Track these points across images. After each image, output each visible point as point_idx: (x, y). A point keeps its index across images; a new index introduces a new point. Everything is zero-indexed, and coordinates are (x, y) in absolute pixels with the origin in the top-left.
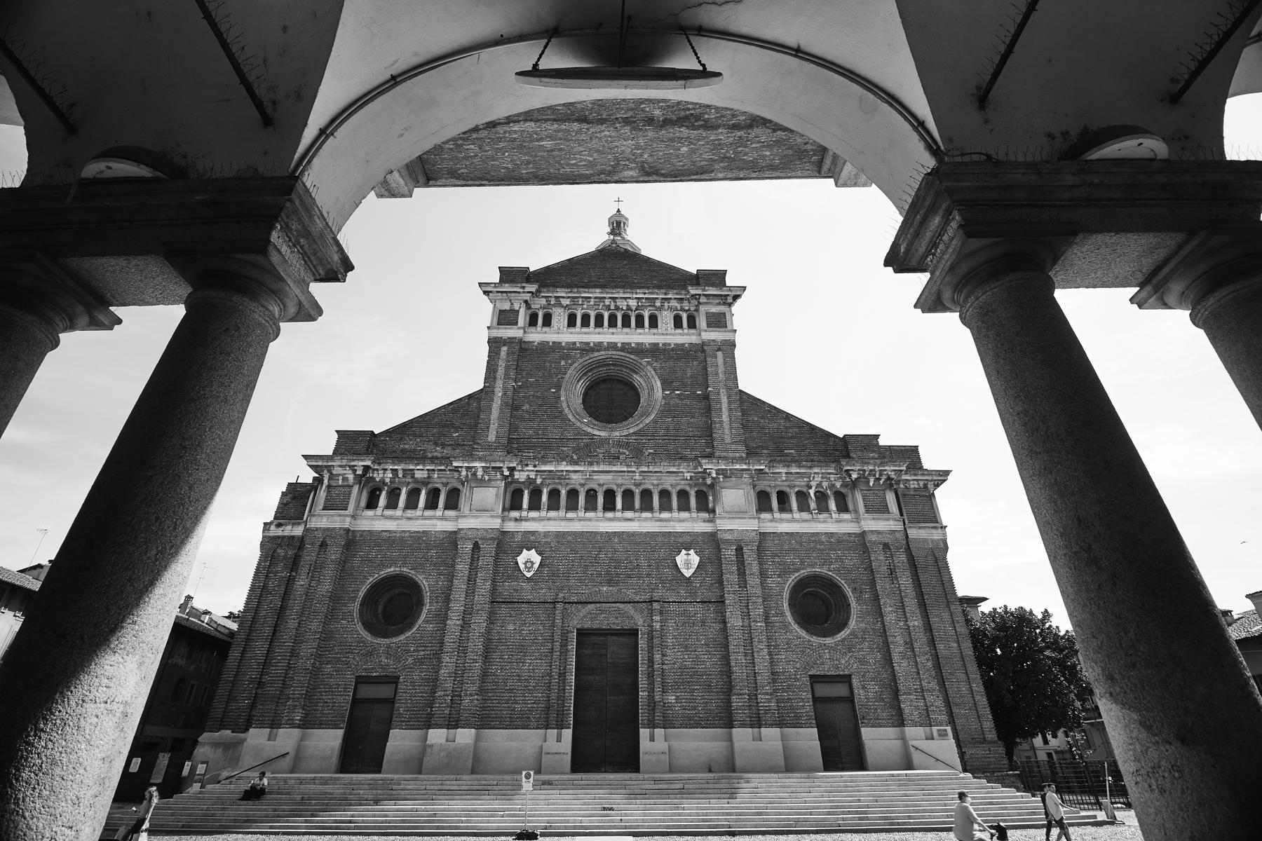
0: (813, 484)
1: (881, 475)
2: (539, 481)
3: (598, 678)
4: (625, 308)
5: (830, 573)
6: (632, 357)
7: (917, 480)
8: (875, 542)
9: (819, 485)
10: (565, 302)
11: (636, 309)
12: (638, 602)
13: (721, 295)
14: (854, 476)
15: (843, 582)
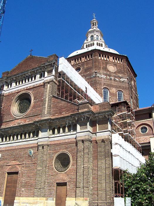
0: (67, 123)
1: (84, 117)
2: (3, 134)
3: (11, 184)
4: (28, 76)
5: (67, 152)
6: (28, 91)
7: (102, 115)
8: (79, 140)
9: (69, 123)
10: (14, 79)
11: (31, 75)
12: (20, 165)
13: (50, 64)
14: (76, 119)
15: (70, 154)
